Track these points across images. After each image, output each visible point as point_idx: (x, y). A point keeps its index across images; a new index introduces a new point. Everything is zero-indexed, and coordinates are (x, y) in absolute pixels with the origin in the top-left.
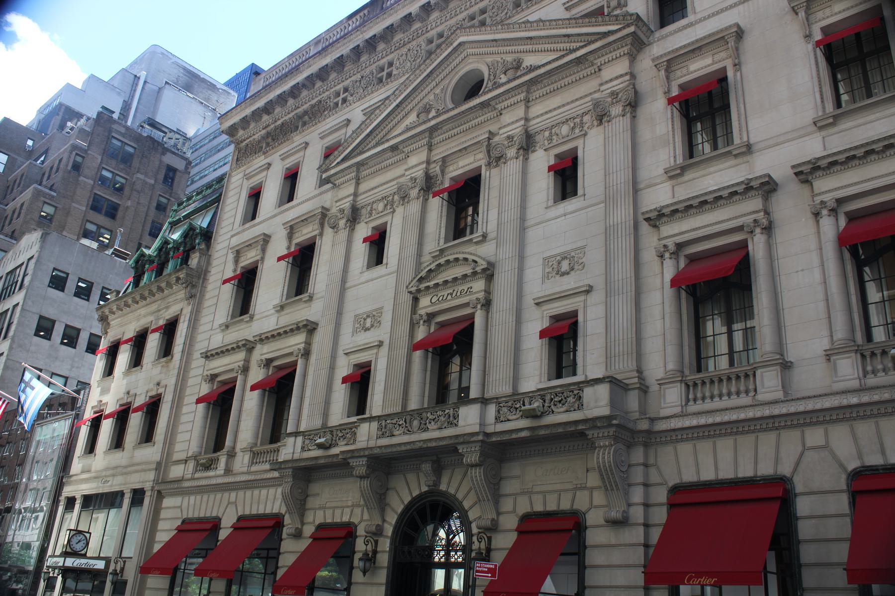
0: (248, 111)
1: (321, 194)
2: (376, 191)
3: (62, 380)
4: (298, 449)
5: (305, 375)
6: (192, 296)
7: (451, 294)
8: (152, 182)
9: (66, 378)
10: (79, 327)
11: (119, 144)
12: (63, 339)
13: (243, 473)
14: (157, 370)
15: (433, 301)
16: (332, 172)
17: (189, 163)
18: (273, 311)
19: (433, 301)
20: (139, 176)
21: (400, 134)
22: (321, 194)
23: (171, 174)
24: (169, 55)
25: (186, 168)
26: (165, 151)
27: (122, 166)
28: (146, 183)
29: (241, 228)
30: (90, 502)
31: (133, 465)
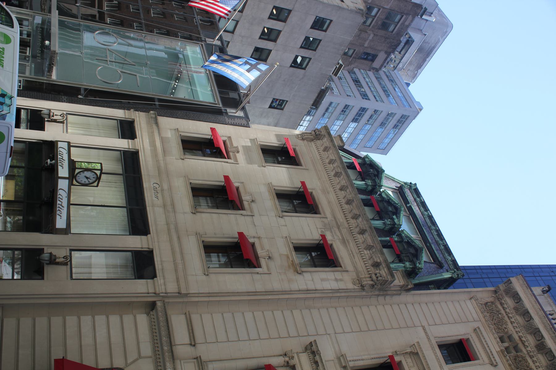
0: (538, 322)
3: (230, 28)
6: (362, 287)
8: (366, 45)
9: (233, 32)
10: (279, 41)
11: (397, 20)
12: (268, 29)
17: (377, 70)
20: (372, 36)
23: (370, 57)
24: (445, 37)
25: (374, 69)
26: (388, 54)
27: (380, 23)
28: (366, 41)
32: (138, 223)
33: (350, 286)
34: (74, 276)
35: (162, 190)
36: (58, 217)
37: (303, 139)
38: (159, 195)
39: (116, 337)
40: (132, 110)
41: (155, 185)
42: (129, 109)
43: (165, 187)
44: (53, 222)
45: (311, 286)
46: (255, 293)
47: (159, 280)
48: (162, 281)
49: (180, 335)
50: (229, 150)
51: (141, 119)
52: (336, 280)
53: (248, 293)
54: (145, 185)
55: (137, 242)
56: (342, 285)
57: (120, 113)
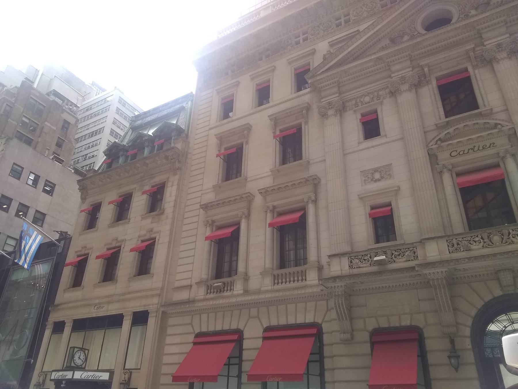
1: (298, 97)
2: (355, 91)
4: (347, 267)
5: (317, 215)
7: (472, 149)
13: (267, 291)
14: (149, 220)
15: (453, 154)
16: (318, 78)
18: (270, 173)
19: (453, 154)
21: (374, 53)
22: (298, 97)
29: (218, 124)
30: (82, 325)
31: (129, 293)
32: (115, 321)
33: (177, 177)
34: (139, 367)
35: (99, 303)
36: (101, 378)
37: (85, 199)
38: (102, 306)
39: (177, 339)
40: (47, 323)
41: (95, 308)
42: (46, 326)
43: (97, 301)
44: (104, 382)
45: (172, 204)
46: (170, 242)
47: (150, 309)
48: (151, 306)
49: (184, 295)
50: (83, 253)
51: (55, 317)
52: (172, 186)
53: (169, 247)
54: (94, 315)
55: (127, 323)
56: (176, 183)
57: (48, 333)
